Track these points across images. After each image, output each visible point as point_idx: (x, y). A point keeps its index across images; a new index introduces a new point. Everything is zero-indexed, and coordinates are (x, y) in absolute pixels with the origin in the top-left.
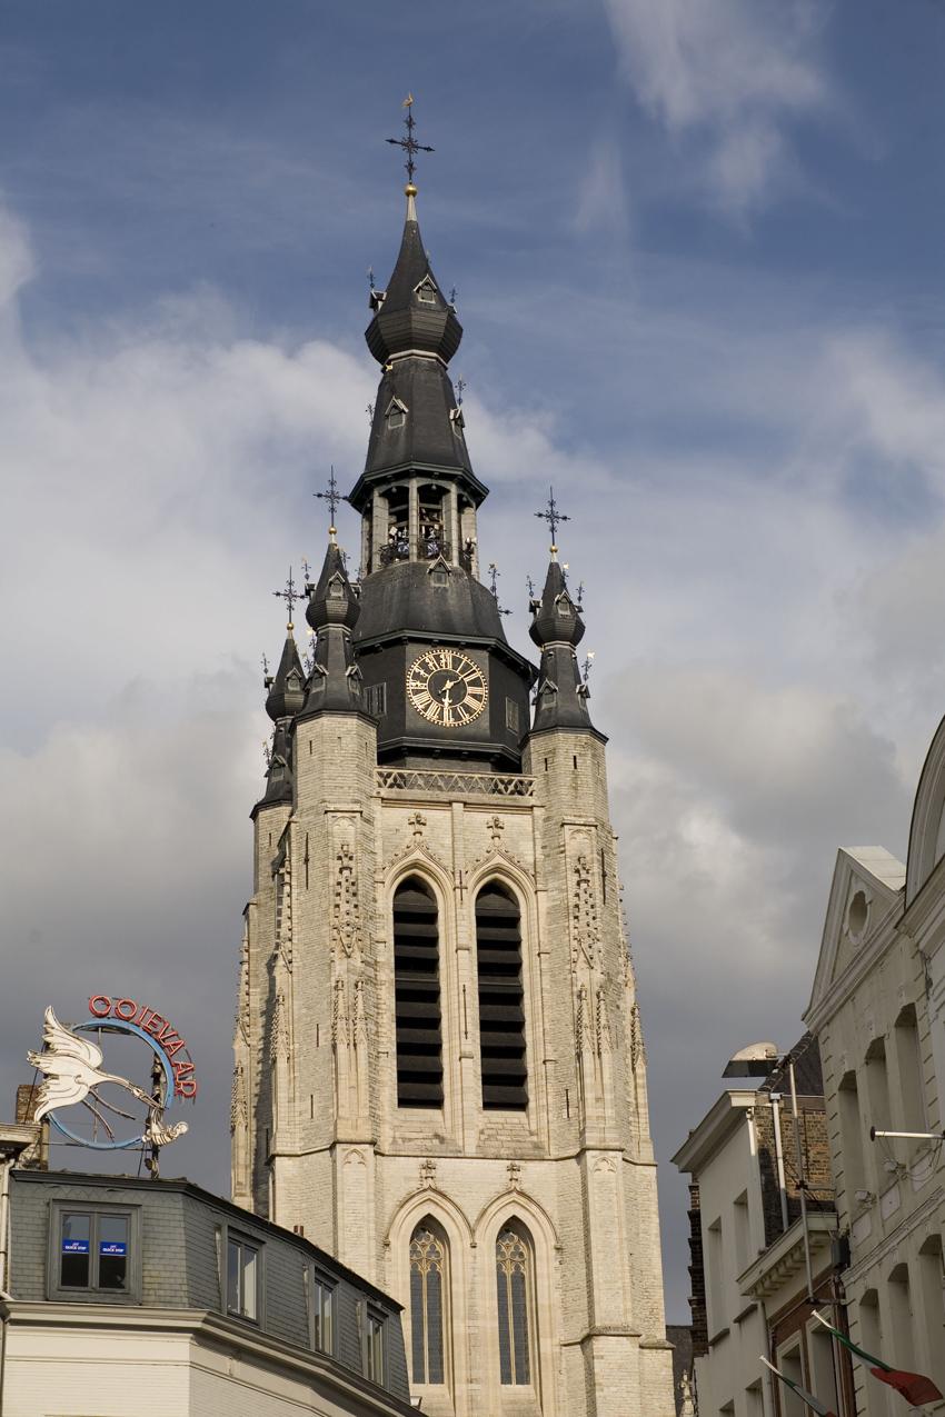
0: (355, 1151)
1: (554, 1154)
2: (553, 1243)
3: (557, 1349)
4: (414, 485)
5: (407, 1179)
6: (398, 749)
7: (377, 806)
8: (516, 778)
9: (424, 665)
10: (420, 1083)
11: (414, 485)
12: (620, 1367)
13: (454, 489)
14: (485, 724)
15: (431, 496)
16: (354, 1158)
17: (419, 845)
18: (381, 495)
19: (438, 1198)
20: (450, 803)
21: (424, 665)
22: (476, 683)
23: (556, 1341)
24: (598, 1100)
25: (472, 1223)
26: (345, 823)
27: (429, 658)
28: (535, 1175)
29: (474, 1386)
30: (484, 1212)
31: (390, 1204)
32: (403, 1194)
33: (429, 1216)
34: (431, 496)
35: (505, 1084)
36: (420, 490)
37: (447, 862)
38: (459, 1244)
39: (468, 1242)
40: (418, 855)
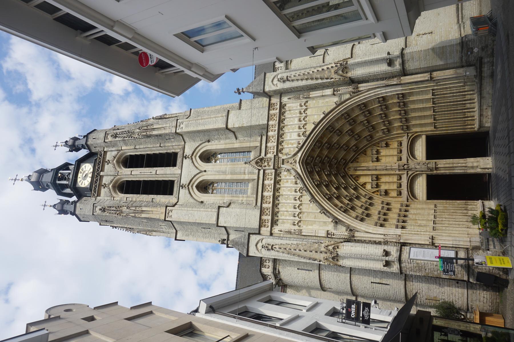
0: (168, 213)
1: (183, 143)
2: (207, 143)
3: (238, 141)
4: (58, 182)
5: (185, 194)
7: (98, 198)
9: (80, 182)
10: (165, 188)
11: (58, 182)
12: (237, 118)
16: (170, 214)
17: (109, 185)
19: (191, 183)
20: (100, 176)
21: (80, 182)
22: (85, 167)
23: (235, 141)
24: (164, 129)
25: (199, 171)
27: (79, 180)
28: (188, 151)
29: (246, 172)
30: (196, 167)
31: (192, 200)
32: (189, 195)
33: (197, 187)
35: (169, 160)
37: (112, 178)
38: (205, 176)
39: (204, 173)
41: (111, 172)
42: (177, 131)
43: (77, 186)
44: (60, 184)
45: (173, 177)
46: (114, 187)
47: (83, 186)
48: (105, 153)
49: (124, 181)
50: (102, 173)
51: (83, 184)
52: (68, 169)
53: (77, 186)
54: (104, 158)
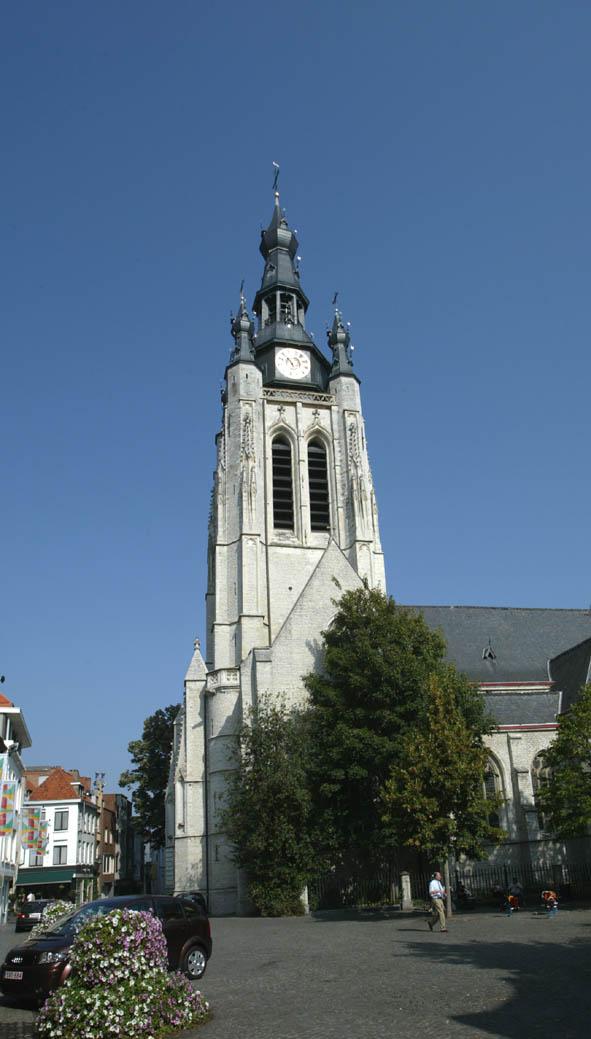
4: (279, 293)
6: (272, 383)
8: (325, 395)
10: (284, 517)
13: (294, 296)
14: (309, 376)
15: (286, 299)
16: (251, 542)
18: (266, 301)
26: (247, 406)
34: (286, 299)
35: (321, 521)
36: (281, 295)
40: (282, 424)
41: (302, 420)
42: (357, 544)
43: (277, 348)
44: (275, 296)
45: (298, 529)
46: (281, 428)
47: (278, 361)
48: (329, 408)
49: (289, 445)
50: (299, 405)
51: (282, 357)
52: (299, 307)
53: (277, 348)
54: (322, 407)
